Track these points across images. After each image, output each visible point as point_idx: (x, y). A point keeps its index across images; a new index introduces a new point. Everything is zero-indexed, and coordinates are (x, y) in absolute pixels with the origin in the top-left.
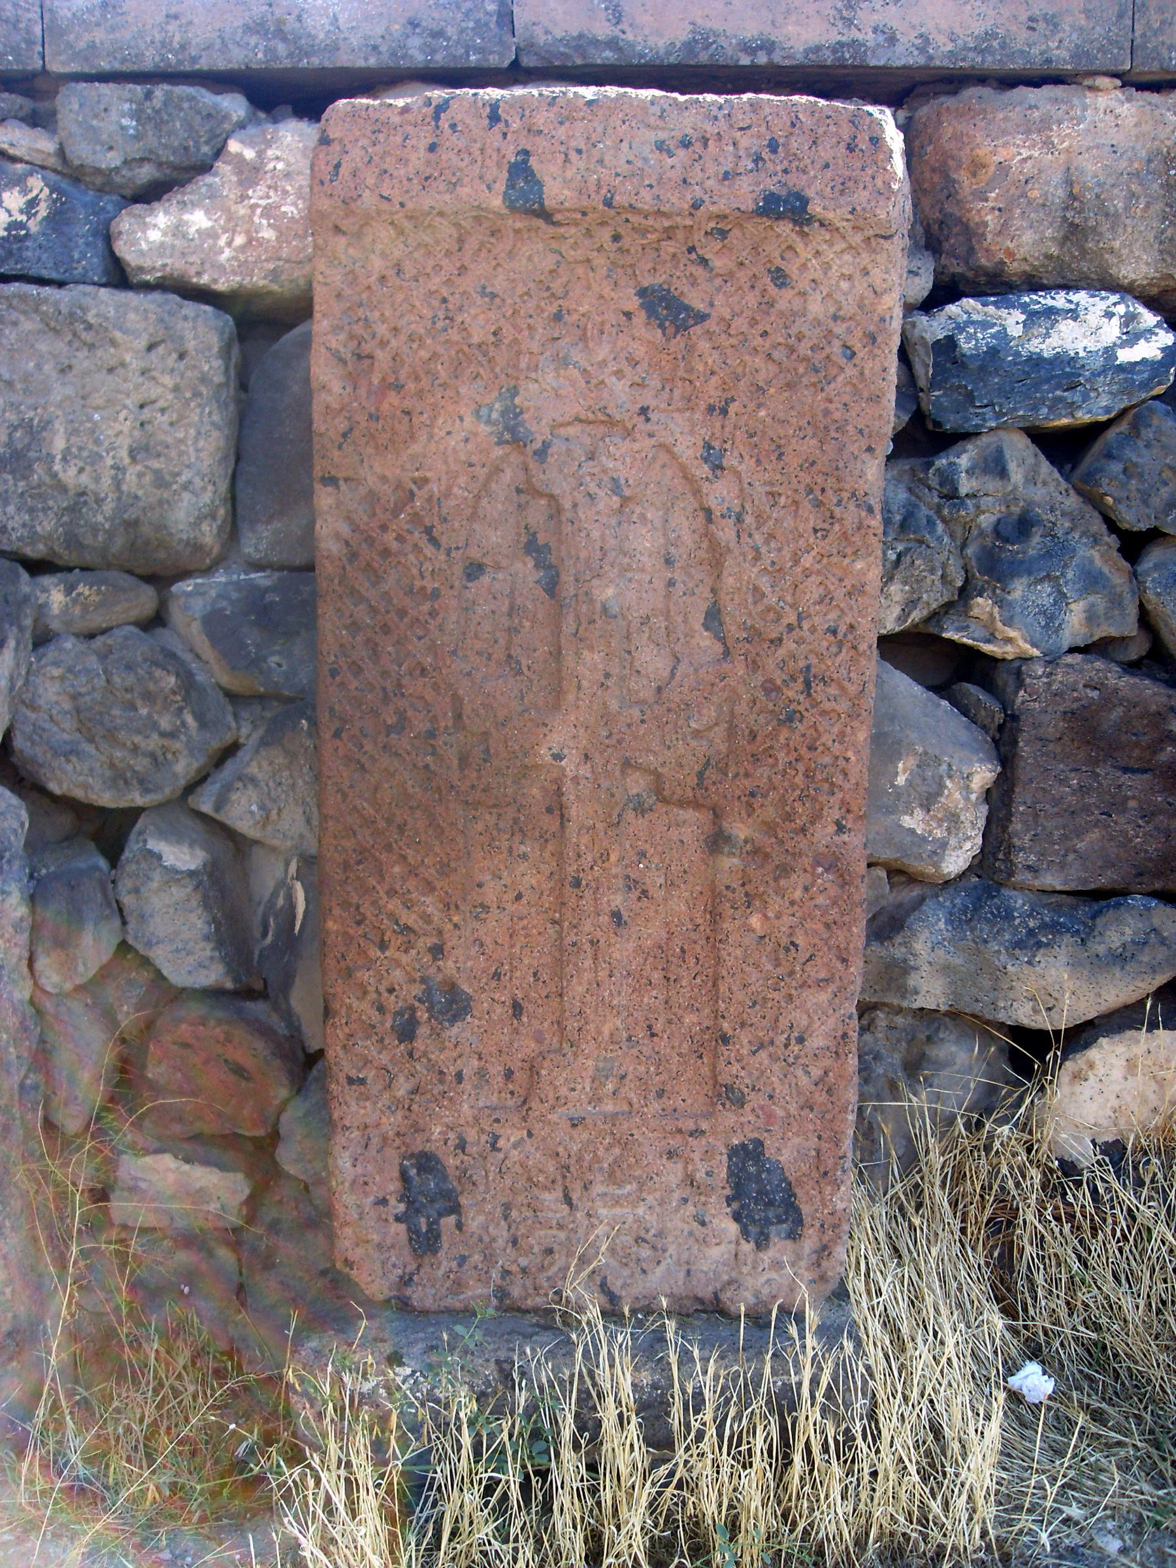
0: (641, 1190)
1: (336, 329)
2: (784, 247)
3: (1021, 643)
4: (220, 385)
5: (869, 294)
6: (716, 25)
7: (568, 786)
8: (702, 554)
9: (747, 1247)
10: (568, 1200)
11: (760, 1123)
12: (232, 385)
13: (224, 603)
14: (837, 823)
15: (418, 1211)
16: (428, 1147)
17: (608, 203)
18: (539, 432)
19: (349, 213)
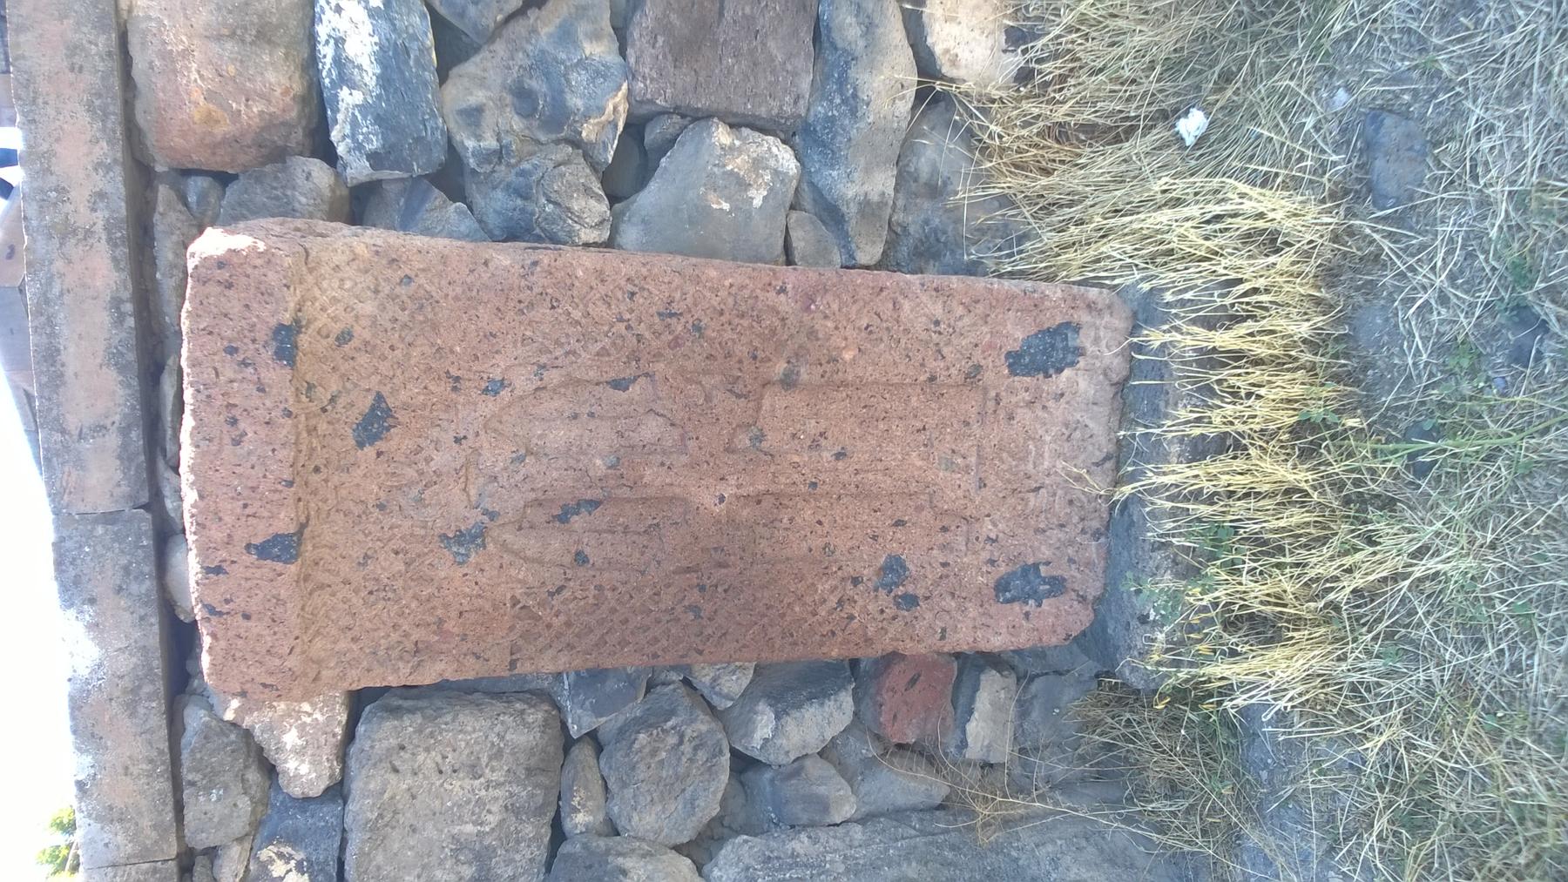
0: (1030, 438)
2: (319, 338)
3: (617, 99)
4: (424, 717)
5: (354, 265)
6: (101, 346)
7: (740, 492)
8: (569, 392)
9: (1082, 363)
11: (995, 353)
12: (421, 704)
14: (779, 293)
15: (1036, 592)
16: (992, 585)
17: (290, 484)
18: (476, 517)
19: (305, 674)
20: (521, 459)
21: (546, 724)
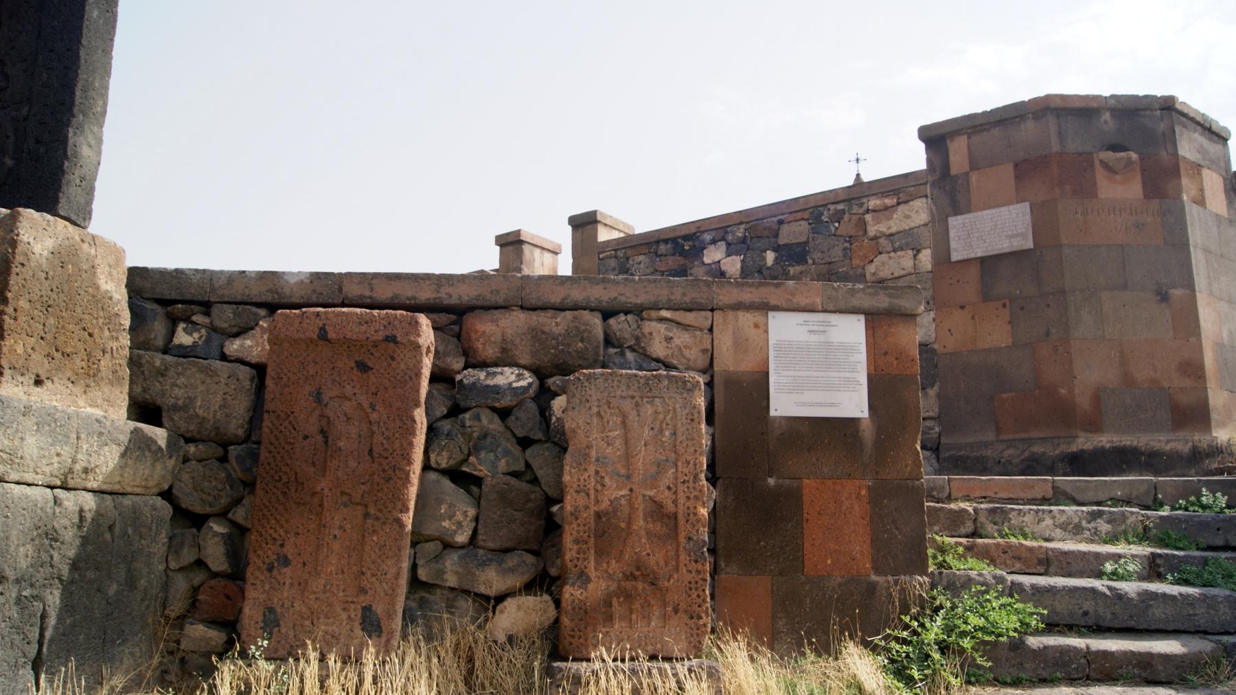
1: (273, 370)
7: (325, 498)
10: (312, 623)
12: (253, 390)
13: (242, 452)
16: (273, 606)
17: (344, 338)
18: (325, 398)
20: (346, 415)
21: (236, 436)
